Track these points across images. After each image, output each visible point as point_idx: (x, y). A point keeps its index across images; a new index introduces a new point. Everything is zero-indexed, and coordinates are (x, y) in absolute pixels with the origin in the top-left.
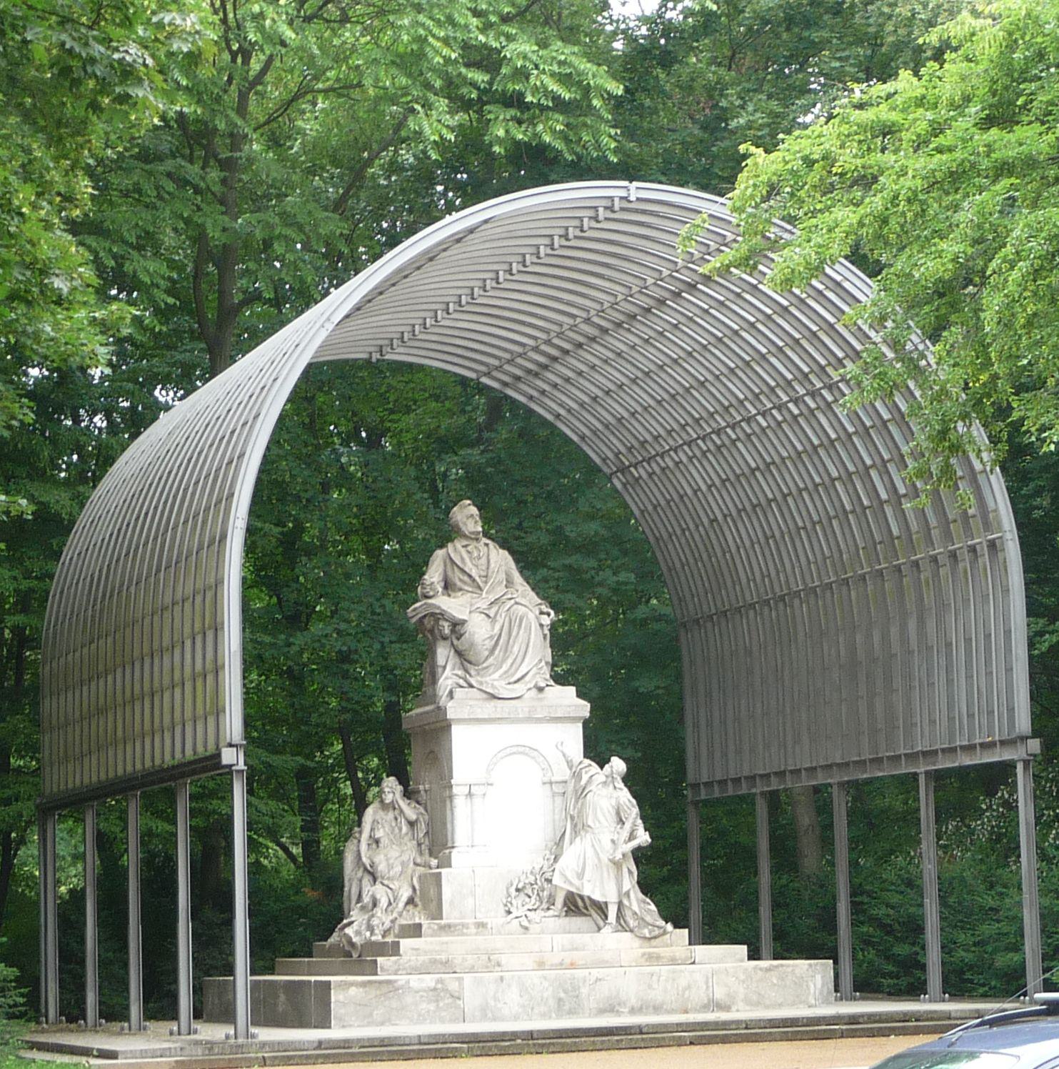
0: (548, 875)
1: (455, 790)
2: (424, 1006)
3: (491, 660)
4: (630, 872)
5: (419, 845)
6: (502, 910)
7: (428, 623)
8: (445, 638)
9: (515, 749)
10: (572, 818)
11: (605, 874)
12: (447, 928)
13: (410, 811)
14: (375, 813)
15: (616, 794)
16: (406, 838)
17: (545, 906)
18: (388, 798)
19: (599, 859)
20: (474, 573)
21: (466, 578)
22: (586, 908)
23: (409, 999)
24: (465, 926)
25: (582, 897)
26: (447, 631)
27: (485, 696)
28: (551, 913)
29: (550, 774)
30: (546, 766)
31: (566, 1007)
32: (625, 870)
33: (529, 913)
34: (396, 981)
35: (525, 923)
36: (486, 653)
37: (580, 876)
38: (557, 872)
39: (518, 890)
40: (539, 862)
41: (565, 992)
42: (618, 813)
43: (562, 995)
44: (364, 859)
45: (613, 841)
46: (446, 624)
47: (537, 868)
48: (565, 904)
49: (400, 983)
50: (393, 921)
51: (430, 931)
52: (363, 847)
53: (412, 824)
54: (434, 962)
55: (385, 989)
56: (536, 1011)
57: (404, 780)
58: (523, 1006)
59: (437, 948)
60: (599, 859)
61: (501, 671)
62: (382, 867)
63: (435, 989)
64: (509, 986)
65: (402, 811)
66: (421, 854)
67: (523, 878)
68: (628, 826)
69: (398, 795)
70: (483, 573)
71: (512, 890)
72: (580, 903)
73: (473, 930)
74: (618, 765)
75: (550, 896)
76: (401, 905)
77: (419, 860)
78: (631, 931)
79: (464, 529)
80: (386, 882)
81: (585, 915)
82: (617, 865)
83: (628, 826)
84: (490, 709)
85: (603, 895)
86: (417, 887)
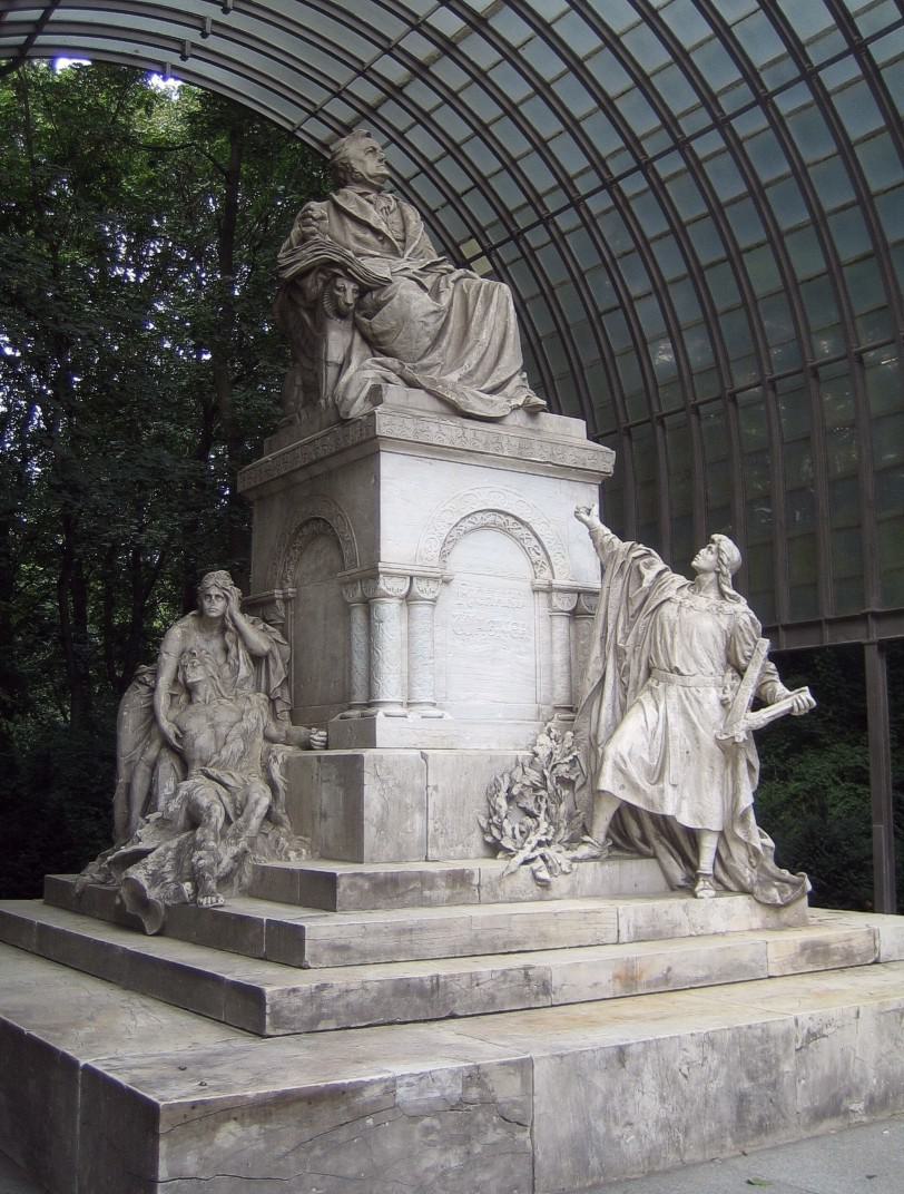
0: (562, 769)
1: (385, 584)
2: (432, 1158)
3: (434, 357)
4: (750, 766)
5: (272, 702)
6: (476, 840)
7: (312, 285)
8: (341, 315)
9: (490, 518)
10: (620, 653)
11: (706, 775)
12: (389, 889)
13: (258, 637)
14: (184, 634)
15: (729, 607)
16: (248, 687)
17: (564, 835)
18: (216, 608)
20: (383, 227)
21: (369, 236)
22: (645, 840)
23: (392, 1145)
24: (425, 880)
26: (350, 298)
27: (437, 406)
28: (584, 851)
29: (546, 574)
31: (753, 1118)
32: (743, 766)
34: (357, 1088)
35: (544, 875)
36: (427, 341)
37: (658, 773)
38: (608, 768)
41: (752, 1077)
43: (746, 1085)
44: (165, 724)
45: (724, 704)
46: (350, 287)
49: (369, 1094)
50: (239, 859)
51: (353, 895)
52: (162, 700)
53: (257, 659)
54: (404, 988)
55: (326, 1116)
56: (694, 1136)
57: (240, 577)
58: (665, 1126)
59: (391, 943)
61: (463, 371)
62: (203, 740)
63: (462, 1102)
64: (637, 1073)
65: (240, 634)
66: (274, 715)
68: (753, 673)
69: (234, 605)
70: (401, 236)
72: (635, 832)
73: (443, 892)
74: (726, 550)
76: (255, 822)
77: (273, 731)
78: (744, 891)
79: (358, 167)
80: (214, 772)
81: (642, 855)
82: (729, 750)
83: (753, 673)
84: (449, 431)
85: (698, 817)
86: (281, 785)
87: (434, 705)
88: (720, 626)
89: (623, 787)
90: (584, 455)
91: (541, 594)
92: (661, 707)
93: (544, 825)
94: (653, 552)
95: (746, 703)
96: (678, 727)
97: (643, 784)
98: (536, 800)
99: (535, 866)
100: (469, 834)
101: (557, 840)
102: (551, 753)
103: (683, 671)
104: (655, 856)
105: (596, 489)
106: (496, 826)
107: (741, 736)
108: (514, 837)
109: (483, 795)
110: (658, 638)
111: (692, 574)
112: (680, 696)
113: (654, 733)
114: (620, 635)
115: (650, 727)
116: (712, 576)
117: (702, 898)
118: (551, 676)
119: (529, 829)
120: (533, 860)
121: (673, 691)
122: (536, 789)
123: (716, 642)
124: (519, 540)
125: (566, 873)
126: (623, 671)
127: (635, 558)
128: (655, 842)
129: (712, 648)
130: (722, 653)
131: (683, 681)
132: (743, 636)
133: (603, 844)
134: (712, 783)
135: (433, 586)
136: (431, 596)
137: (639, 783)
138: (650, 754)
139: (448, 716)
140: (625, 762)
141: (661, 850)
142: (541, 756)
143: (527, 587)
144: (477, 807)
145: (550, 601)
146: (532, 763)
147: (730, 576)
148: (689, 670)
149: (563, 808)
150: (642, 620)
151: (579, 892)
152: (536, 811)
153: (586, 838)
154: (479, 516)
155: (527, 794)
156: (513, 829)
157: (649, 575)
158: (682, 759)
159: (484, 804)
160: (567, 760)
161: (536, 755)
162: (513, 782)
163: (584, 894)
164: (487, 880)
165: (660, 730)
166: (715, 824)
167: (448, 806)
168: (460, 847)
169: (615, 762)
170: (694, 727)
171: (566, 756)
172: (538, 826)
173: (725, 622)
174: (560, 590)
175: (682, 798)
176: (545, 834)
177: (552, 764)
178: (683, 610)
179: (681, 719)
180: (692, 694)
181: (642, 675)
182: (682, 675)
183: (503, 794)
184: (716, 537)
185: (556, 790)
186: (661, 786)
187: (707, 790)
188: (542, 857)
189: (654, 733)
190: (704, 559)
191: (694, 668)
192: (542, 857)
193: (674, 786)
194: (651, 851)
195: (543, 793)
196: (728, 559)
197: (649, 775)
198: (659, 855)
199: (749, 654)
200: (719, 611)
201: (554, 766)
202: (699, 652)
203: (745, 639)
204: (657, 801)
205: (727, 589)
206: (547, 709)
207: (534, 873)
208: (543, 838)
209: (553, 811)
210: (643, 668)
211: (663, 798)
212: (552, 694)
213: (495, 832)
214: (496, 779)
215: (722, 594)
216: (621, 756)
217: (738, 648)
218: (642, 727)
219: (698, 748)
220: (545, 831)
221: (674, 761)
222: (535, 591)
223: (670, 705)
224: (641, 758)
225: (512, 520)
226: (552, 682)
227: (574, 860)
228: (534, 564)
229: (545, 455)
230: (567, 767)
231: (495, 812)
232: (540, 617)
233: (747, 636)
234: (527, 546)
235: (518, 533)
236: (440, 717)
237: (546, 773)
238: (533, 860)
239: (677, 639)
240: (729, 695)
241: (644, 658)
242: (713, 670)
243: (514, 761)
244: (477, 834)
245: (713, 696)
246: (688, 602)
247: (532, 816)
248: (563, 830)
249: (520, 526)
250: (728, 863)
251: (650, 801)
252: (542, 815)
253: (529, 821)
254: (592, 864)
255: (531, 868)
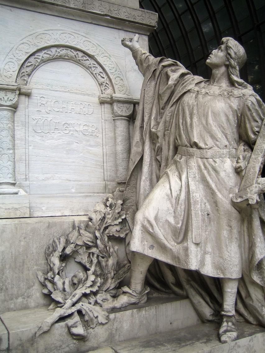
0: (113, 230)
6: (36, 293)
9: (64, 52)
10: (154, 138)
11: (225, 233)
15: (237, 92)
17: (111, 284)
19: (215, 203)
25: (171, 268)
28: (123, 300)
30: (106, 80)
33: (85, 306)
35: (79, 330)
37: (182, 233)
38: (137, 231)
39: (64, 258)
40: (96, 208)
42: (241, 126)
45: (238, 171)
47: (96, 218)
48: (147, 283)
60: (215, 203)
67: (73, 237)
71: (56, 261)
72: (170, 278)
75: (119, 266)
85: (218, 267)
87: (14, 184)
88: (231, 107)
89: (152, 247)
90: (134, 13)
91: (106, 105)
92: (184, 177)
93: (92, 278)
94: (178, 63)
95: (257, 169)
96: (198, 193)
97: (171, 244)
98: (89, 256)
99: (70, 322)
100: (29, 288)
101: (105, 289)
102: (104, 218)
103: (202, 145)
104: (187, 297)
105: (146, 38)
106: (50, 281)
107: (254, 198)
108: (64, 290)
109: (42, 255)
110: (181, 121)
111: (207, 73)
112: (199, 167)
113: (178, 198)
114: (153, 123)
115: (175, 194)
116: (223, 69)
117: (225, 342)
118: (116, 161)
119: (80, 282)
120: (70, 316)
121: (193, 163)
122: (88, 247)
123: (228, 119)
124: (88, 68)
125: (102, 324)
126: (157, 152)
127: (164, 67)
128: (187, 287)
129: (225, 125)
130: (235, 130)
131: (201, 154)
132: (251, 114)
133: (141, 293)
134: (230, 239)
135: (11, 96)
136: (9, 103)
137: (166, 242)
138: (175, 217)
139: (22, 192)
140: (152, 225)
141: (192, 293)
142: (94, 220)
143: (96, 100)
144: (37, 265)
145: (113, 109)
146: (87, 226)
147: (238, 68)
148: (206, 144)
149: (111, 262)
150: (168, 111)
151: (117, 337)
152: (88, 266)
153: (126, 289)
154: (54, 50)
155: (81, 251)
156: (64, 283)
157: (174, 76)
158: (203, 220)
159: (43, 262)
160: (117, 222)
161: (91, 219)
162: (68, 242)
163: (122, 338)
164: (17, 343)
165: (183, 196)
166: (234, 271)
167: (7, 266)
168: (20, 300)
169: (143, 226)
170: (213, 193)
171: (116, 219)
172: (87, 279)
173: (235, 103)
174: (119, 101)
175: (205, 253)
176: (91, 286)
177: (104, 226)
178: (200, 96)
179: (201, 186)
180: (210, 164)
181: (171, 153)
182: (200, 148)
183: (57, 254)
184: (224, 39)
185: (106, 247)
186: (185, 244)
187: (226, 246)
188: (80, 312)
189: (178, 198)
190: (216, 56)
191: (210, 142)
192: (80, 312)
193: (197, 244)
194: (185, 293)
195: (94, 250)
196: (235, 53)
197: (175, 235)
198: (191, 297)
199: (257, 129)
200: (230, 95)
201: (106, 228)
202: (214, 128)
203: (253, 117)
204: (182, 257)
205: (235, 78)
206: (111, 185)
207: (69, 328)
208: (88, 291)
209: (104, 264)
210: (171, 147)
211: (187, 255)
212: (116, 173)
213: (49, 285)
214: (54, 241)
215: (232, 83)
216: (149, 222)
217: (248, 125)
218: (168, 196)
219: (217, 210)
220: (91, 283)
221: (196, 222)
222: (102, 103)
223: (191, 175)
224: (167, 221)
225: (80, 54)
226: (116, 166)
227: (114, 310)
228: (101, 84)
229: (104, 10)
230: (118, 228)
231: (51, 269)
232: (106, 120)
233: (254, 114)
234: (94, 73)
235: (87, 63)
236: (17, 193)
237: (98, 234)
238: (70, 316)
239: (195, 119)
240: (242, 164)
241: (172, 140)
242: (227, 143)
243: (71, 226)
244: (37, 287)
245: (227, 166)
246: (203, 91)
247: (86, 269)
248: (110, 281)
249: (88, 58)
250: (248, 301)
251: (176, 258)
252: (92, 269)
253: (81, 275)
254: (128, 313)
255: (67, 325)
